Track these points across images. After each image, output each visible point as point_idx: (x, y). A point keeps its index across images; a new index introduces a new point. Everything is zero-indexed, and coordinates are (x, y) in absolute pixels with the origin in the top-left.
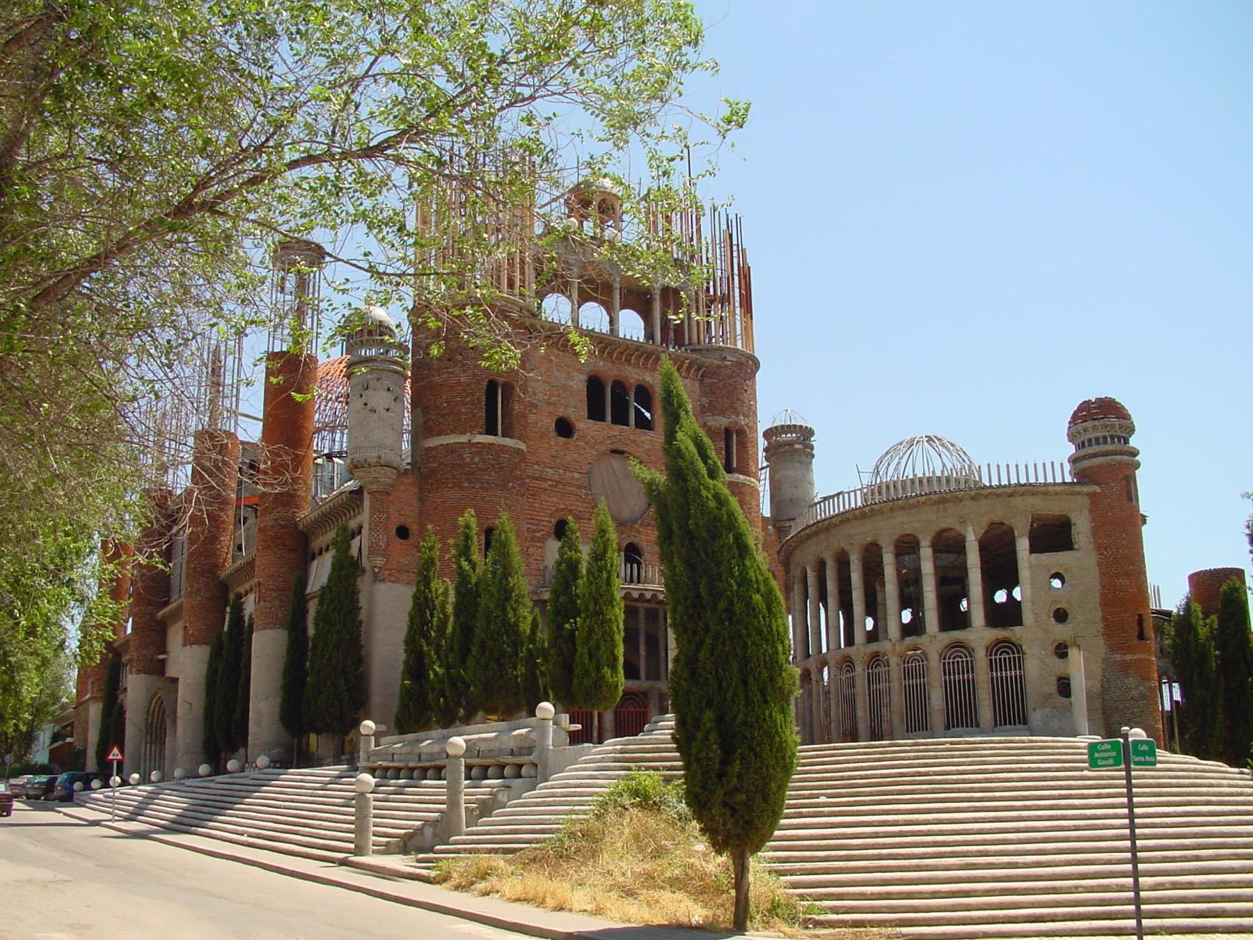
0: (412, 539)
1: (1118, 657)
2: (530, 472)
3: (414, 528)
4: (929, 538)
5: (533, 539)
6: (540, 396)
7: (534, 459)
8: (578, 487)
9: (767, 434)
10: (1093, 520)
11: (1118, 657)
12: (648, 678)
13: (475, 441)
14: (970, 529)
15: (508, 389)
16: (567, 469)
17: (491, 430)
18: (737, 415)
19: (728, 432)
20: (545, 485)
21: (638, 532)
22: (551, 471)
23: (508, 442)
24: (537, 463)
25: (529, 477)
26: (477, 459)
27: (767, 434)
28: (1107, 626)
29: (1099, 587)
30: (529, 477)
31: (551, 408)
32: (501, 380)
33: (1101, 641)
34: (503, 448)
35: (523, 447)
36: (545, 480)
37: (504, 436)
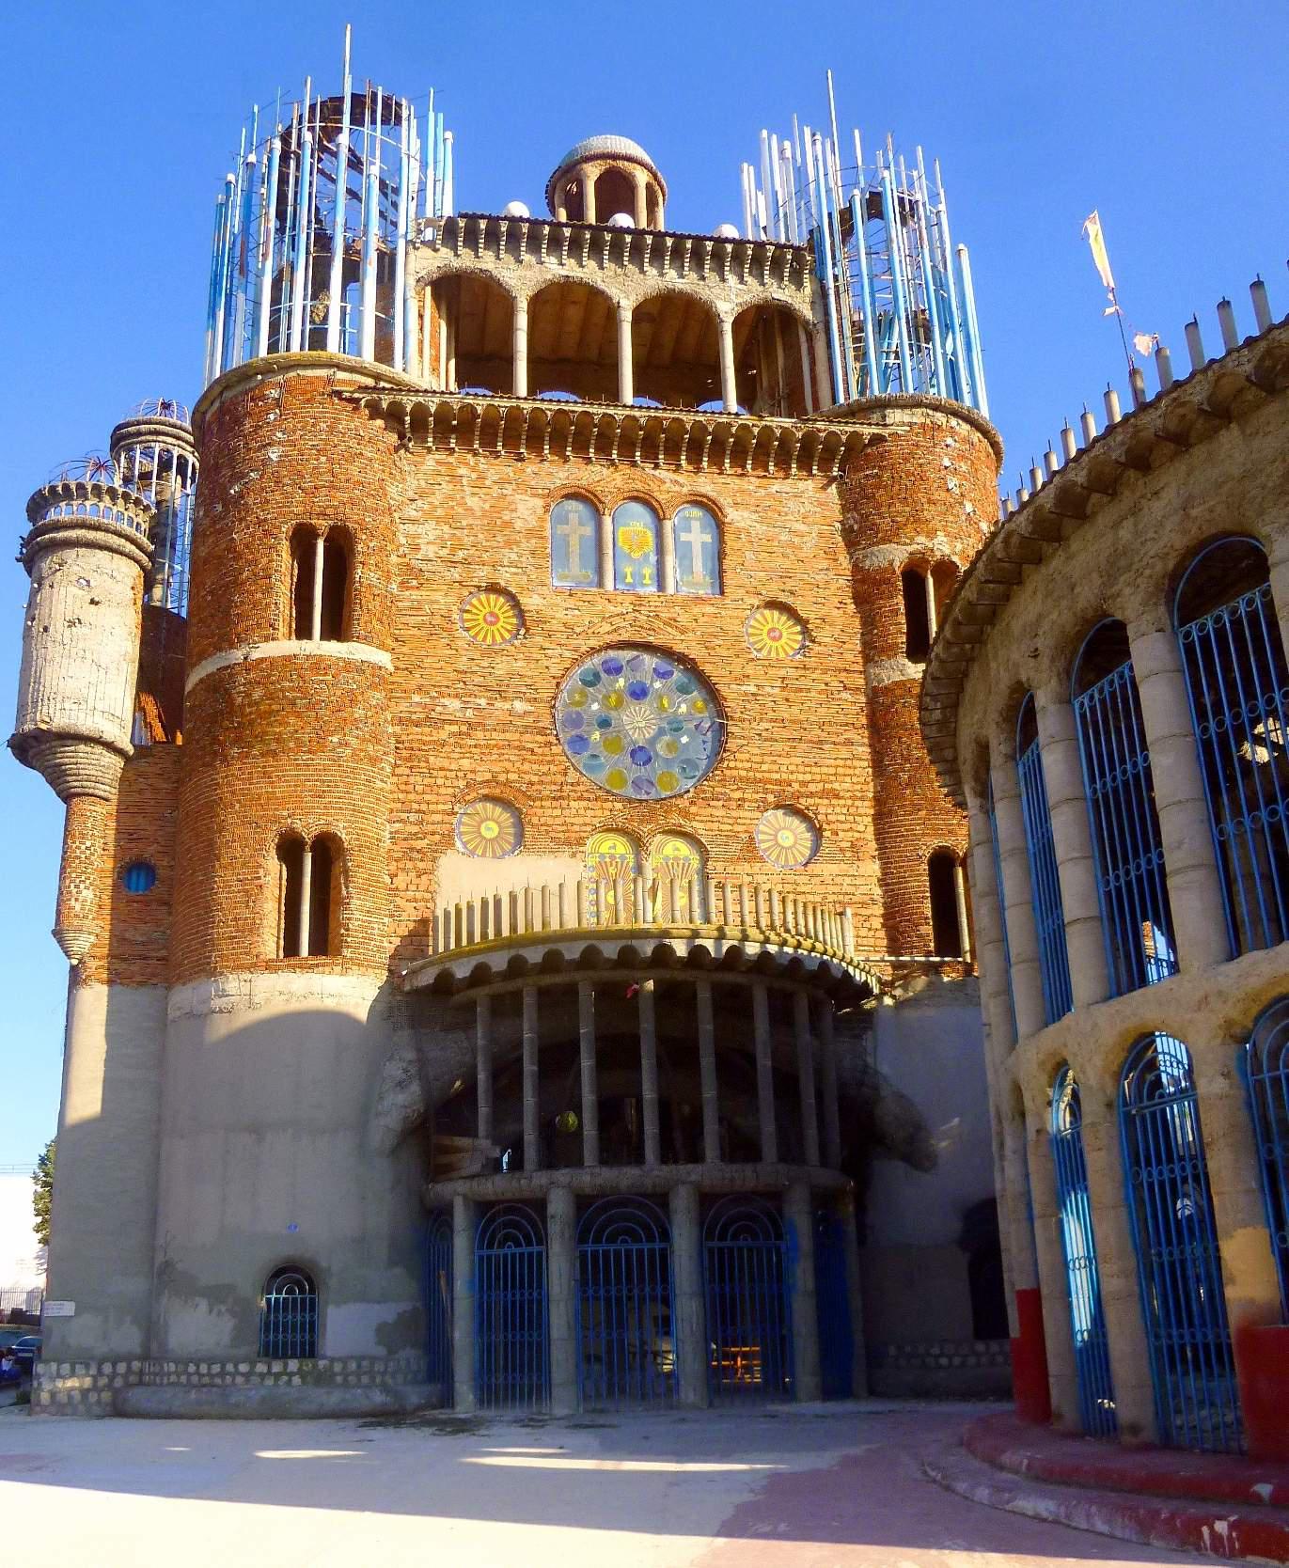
3: (162, 864)
5: (409, 853)
6: (431, 551)
7: (416, 679)
8: (526, 730)
12: (667, 1155)
13: (256, 655)
17: (303, 631)
18: (931, 534)
20: (443, 735)
21: (685, 814)
22: (454, 704)
23: (333, 648)
24: (420, 689)
25: (400, 721)
26: (256, 695)
31: (456, 574)
32: (323, 525)
34: (318, 664)
35: (383, 659)
37: (326, 635)
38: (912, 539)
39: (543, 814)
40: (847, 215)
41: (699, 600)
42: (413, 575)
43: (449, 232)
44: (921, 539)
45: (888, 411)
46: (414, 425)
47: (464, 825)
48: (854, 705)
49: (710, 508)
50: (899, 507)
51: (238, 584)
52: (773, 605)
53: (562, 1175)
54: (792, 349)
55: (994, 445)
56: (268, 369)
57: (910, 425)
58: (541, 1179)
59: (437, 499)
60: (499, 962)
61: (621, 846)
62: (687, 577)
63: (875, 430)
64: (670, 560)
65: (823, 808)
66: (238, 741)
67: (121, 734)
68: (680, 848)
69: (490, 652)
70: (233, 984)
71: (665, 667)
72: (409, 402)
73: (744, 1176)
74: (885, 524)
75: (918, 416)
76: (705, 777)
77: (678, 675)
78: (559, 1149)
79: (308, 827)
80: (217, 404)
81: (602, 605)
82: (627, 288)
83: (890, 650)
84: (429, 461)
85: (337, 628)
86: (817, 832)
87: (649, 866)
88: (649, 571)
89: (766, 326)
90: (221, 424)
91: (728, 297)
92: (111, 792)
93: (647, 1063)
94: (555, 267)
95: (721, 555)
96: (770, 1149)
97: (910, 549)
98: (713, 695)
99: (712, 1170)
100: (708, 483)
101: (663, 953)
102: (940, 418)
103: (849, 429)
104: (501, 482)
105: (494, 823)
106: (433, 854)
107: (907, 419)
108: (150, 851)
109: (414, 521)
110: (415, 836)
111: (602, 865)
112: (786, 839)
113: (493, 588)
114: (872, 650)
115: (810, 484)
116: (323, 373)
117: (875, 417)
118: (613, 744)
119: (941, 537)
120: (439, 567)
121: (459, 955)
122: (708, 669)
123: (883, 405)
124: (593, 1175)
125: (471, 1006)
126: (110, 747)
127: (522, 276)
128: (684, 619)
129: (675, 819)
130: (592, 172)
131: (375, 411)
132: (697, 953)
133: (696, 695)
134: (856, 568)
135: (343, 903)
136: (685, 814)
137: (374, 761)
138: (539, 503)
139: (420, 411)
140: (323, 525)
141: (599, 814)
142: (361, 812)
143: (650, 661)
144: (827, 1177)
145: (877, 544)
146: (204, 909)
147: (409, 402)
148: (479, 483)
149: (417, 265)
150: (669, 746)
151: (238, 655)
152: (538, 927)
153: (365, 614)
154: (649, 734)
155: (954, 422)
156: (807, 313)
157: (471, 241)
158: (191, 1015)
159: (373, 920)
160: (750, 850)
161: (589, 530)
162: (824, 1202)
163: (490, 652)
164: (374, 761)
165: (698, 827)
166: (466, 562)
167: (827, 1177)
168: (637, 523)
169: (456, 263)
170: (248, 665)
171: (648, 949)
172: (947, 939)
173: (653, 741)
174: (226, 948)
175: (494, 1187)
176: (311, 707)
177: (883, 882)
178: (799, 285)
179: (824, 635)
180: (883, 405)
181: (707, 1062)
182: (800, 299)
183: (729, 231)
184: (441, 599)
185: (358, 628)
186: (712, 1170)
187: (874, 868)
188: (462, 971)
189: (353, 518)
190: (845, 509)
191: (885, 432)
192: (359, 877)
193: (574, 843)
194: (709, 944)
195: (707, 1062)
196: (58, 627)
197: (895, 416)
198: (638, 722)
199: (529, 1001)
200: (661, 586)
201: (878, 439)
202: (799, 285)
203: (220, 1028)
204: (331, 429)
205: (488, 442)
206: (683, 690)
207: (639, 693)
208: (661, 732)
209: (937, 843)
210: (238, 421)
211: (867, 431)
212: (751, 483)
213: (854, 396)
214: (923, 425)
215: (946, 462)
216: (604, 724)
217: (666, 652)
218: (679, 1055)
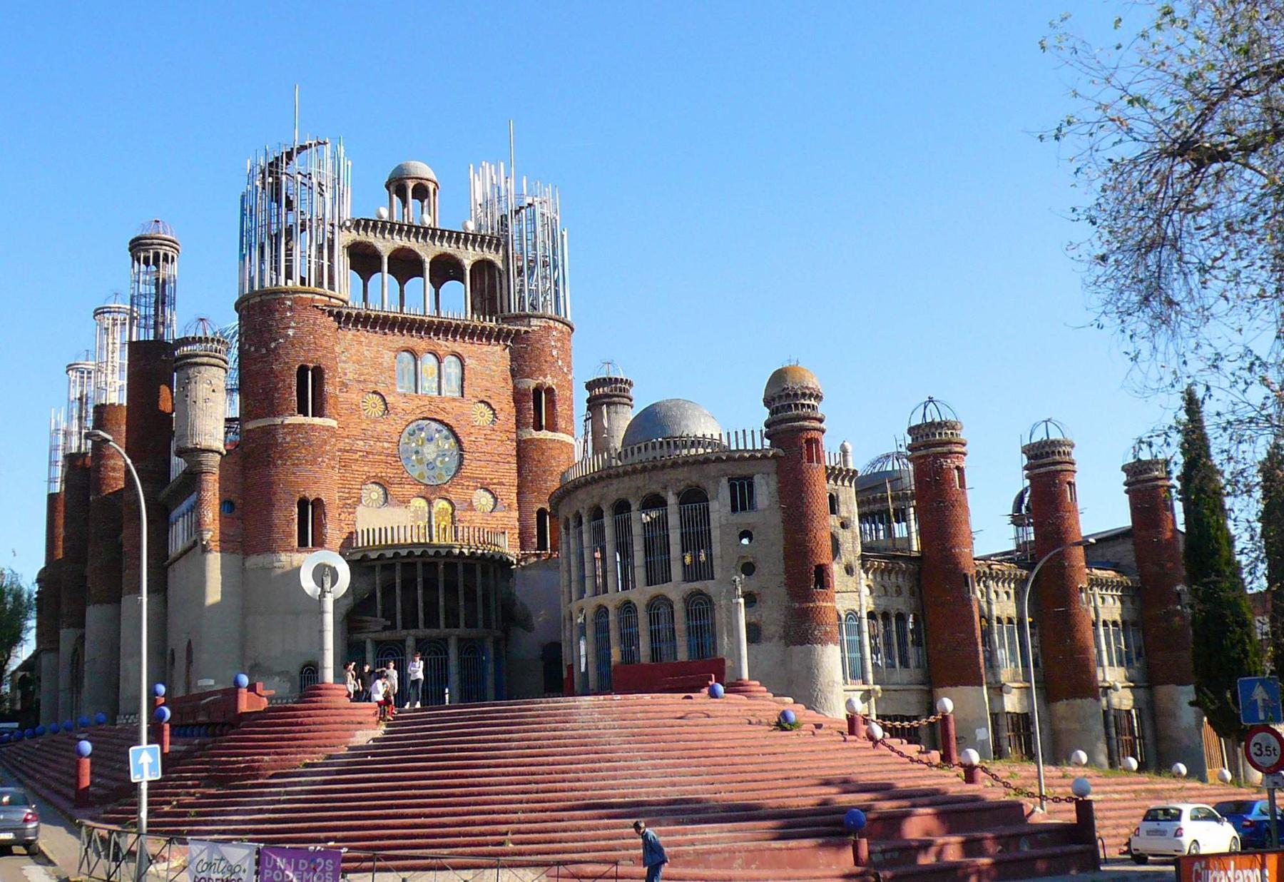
0: (237, 513)
2: (341, 445)
5: (345, 506)
6: (350, 376)
9: (590, 386)
10: (779, 482)
13: (286, 422)
14: (670, 494)
15: (318, 373)
16: (378, 440)
17: (303, 411)
18: (545, 377)
19: (537, 392)
21: (447, 491)
22: (361, 443)
23: (317, 421)
24: (348, 437)
25: (340, 450)
27: (590, 386)
28: (788, 578)
29: (783, 542)
30: (340, 450)
32: (311, 365)
33: (783, 591)
34: (313, 427)
35: (334, 423)
36: (356, 452)
39: (394, 490)
41: (454, 400)
42: (344, 385)
43: (357, 224)
46: (344, 319)
47: (364, 493)
48: (511, 448)
49: (460, 357)
51: (277, 389)
52: (482, 402)
53: (412, 632)
54: (492, 277)
56: (287, 292)
58: (404, 632)
59: (353, 351)
60: (389, 554)
61: (423, 503)
62: (450, 389)
64: (443, 381)
65: (498, 489)
66: (280, 458)
67: (220, 445)
68: (445, 504)
69: (375, 421)
70: (284, 557)
71: (440, 427)
72: (345, 311)
73: (473, 633)
74: (527, 369)
75: (542, 323)
76: (454, 476)
77: (445, 432)
78: (410, 622)
79: (311, 496)
80: (258, 299)
81: (417, 401)
82: (427, 252)
83: (526, 425)
84: (350, 334)
85: (318, 412)
86: (496, 499)
87: (434, 511)
88: (435, 385)
89: (482, 267)
90: (261, 308)
91: (469, 256)
92: (216, 470)
93: (441, 592)
94: (399, 241)
95: (463, 379)
96: (481, 623)
98: (458, 441)
99: (461, 631)
100: (460, 346)
101: (449, 554)
104: (378, 345)
105: (376, 493)
106: (354, 506)
108: (233, 497)
109: (345, 362)
110: (347, 498)
111: (416, 511)
112: (484, 501)
113: (375, 392)
114: (520, 424)
115: (498, 348)
116: (309, 296)
118: (420, 461)
120: (355, 384)
121: (374, 548)
122: (457, 430)
123: (530, 316)
124: (422, 632)
125: (373, 568)
126: (220, 453)
127: (385, 245)
128: (449, 409)
129: (444, 493)
130: (411, 185)
131: (330, 313)
132: (462, 553)
133: (452, 440)
134: (515, 387)
135: (324, 526)
136: (447, 491)
137: (333, 468)
138: (393, 354)
139: (349, 315)
140: (311, 365)
141: (416, 490)
142: (325, 484)
143: (434, 425)
144: (499, 633)
146: (268, 526)
147: (345, 311)
148: (369, 344)
149: (344, 239)
150: (442, 462)
151: (278, 421)
152: (402, 541)
153: (328, 409)
154: (434, 456)
156: (500, 264)
157: (365, 229)
158: (263, 568)
159: (334, 534)
160: (471, 507)
161: (412, 367)
162: (497, 642)
163: (375, 421)
164: (333, 468)
165: (452, 497)
166: (365, 381)
167: (499, 633)
168: (429, 362)
169: (358, 239)
170: (283, 426)
171: (443, 552)
172: (541, 545)
173: (435, 460)
174: (280, 543)
175: (386, 635)
176: (311, 446)
177: (519, 520)
178: (497, 251)
179: (501, 416)
180: (530, 316)
181: (461, 593)
182: (496, 258)
183: (471, 227)
184: (354, 397)
185: (327, 412)
186: (461, 631)
187: (516, 514)
188: (374, 555)
189: (324, 363)
190: (512, 360)
192: (329, 515)
193: (405, 502)
194: (466, 551)
195: (461, 593)
196: (200, 403)
197: (534, 322)
198: (430, 451)
199: (398, 567)
200: (440, 393)
201: (526, 332)
202: (497, 251)
203: (279, 571)
204: (314, 324)
205: (373, 327)
206: (447, 438)
207: (430, 440)
208: (438, 456)
209: (540, 506)
210: (272, 311)
211: (523, 329)
212: (475, 348)
216: (417, 452)
217: (441, 422)
218: (451, 588)
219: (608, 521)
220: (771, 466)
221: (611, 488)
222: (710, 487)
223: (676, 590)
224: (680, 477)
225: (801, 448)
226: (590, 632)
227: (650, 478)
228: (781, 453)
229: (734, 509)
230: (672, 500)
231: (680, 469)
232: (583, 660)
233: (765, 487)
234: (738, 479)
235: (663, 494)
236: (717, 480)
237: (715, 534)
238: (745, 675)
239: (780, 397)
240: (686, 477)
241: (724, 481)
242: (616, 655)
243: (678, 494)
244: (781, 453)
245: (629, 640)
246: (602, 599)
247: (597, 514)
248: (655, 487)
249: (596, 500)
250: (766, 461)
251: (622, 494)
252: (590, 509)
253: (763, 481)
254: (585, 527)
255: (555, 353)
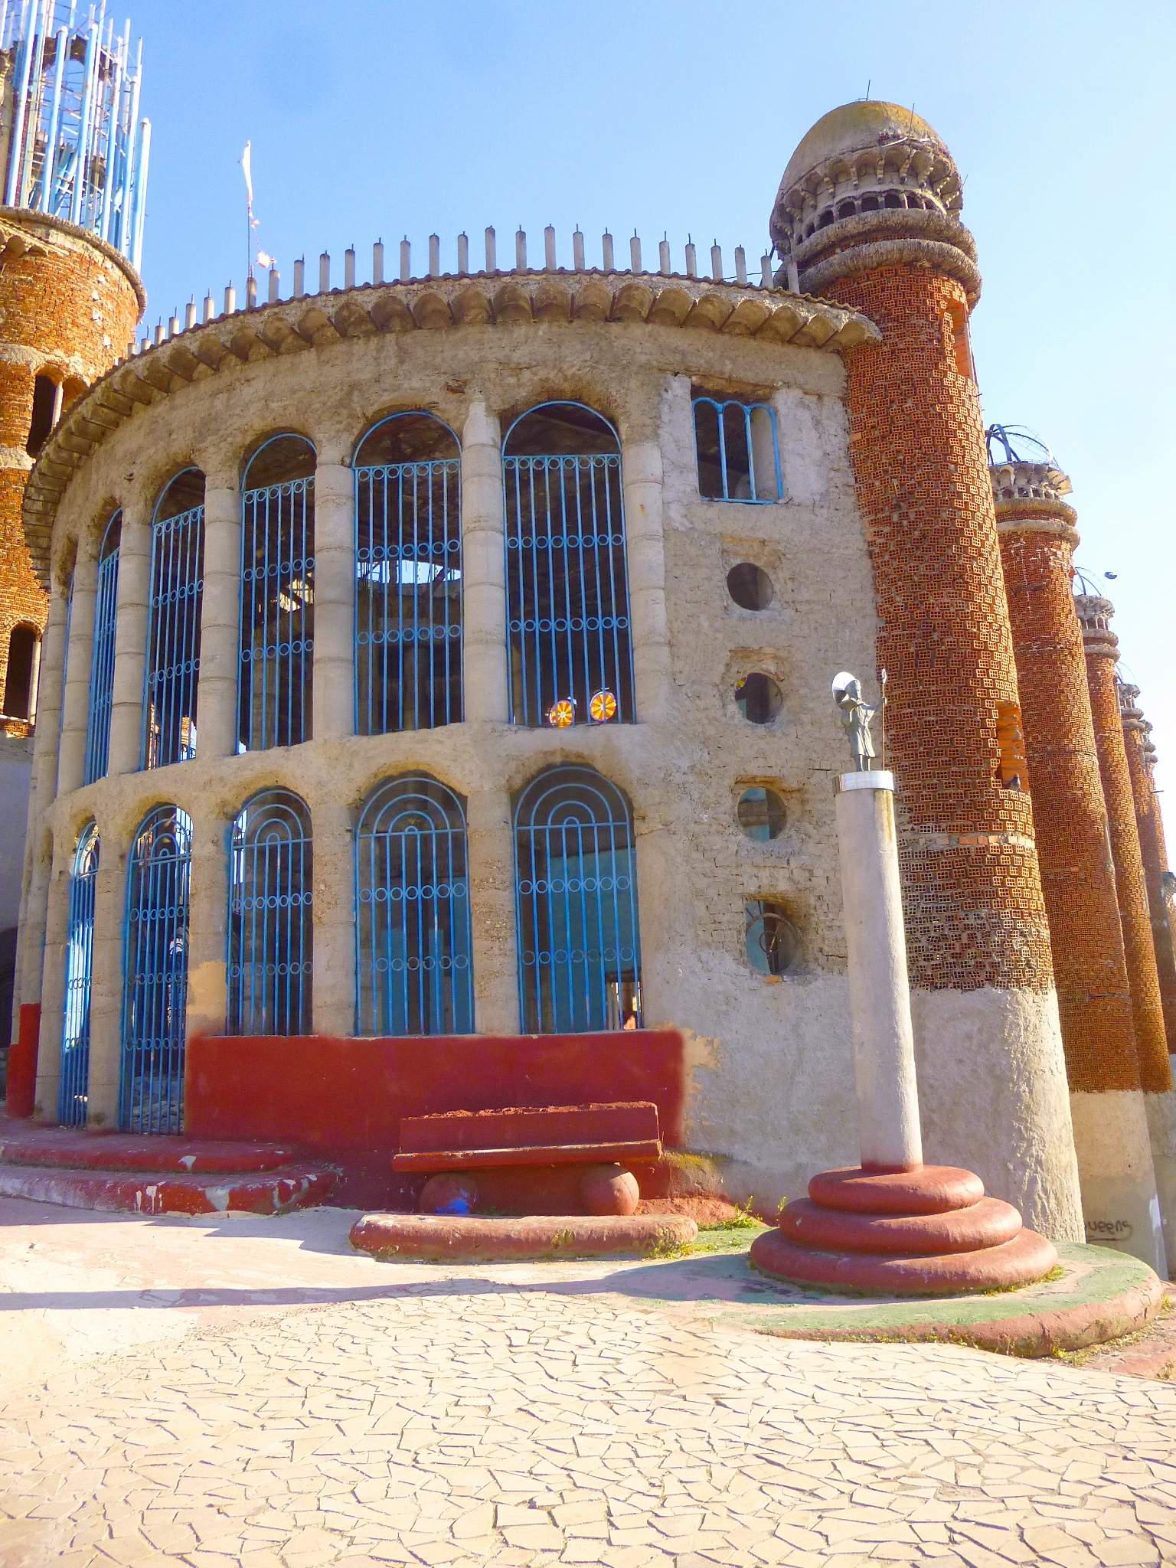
1: (940, 841)
4: (348, 439)
10: (855, 425)
11: (940, 841)
18: (69, 352)
38: (51, 350)
40: (51, 45)
44: (59, 352)
45: (52, 231)
50: (45, 317)
55: (140, 297)
57: (70, 251)
63: (39, 244)
74: (29, 328)
75: (78, 246)
97: (49, 357)
102: (97, 256)
103: (13, 232)
107: (68, 245)
117: (40, 232)
119: (77, 357)
123: (50, 224)
145: (15, 342)
155: (109, 264)
191: (47, 249)
197: (56, 237)
201: (36, 251)
209: (22, 617)
211: (30, 241)
213: (25, 205)
214: (81, 256)
215: (95, 295)
219: (220, 510)
220: (827, 371)
221: (247, 392)
222: (630, 406)
223: (477, 753)
224: (520, 356)
225: (938, 319)
226: (110, 901)
227: (403, 355)
228: (872, 331)
229: (709, 488)
230: (480, 433)
231: (521, 331)
232: (75, 999)
233: (809, 435)
234: (720, 396)
235: (447, 410)
236: (657, 374)
237: (646, 561)
238: (915, 1151)
239: (865, 168)
240: (544, 358)
241: (679, 389)
242: (205, 995)
243: (505, 418)
244: (872, 331)
245: (277, 942)
246: (161, 782)
247: (183, 488)
248: (417, 386)
249: (180, 443)
250: (815, 357)
251: (281, 412)
252: (157, 479)
253: (805, 416)
254: (130, 538)
255: (97, 314)
